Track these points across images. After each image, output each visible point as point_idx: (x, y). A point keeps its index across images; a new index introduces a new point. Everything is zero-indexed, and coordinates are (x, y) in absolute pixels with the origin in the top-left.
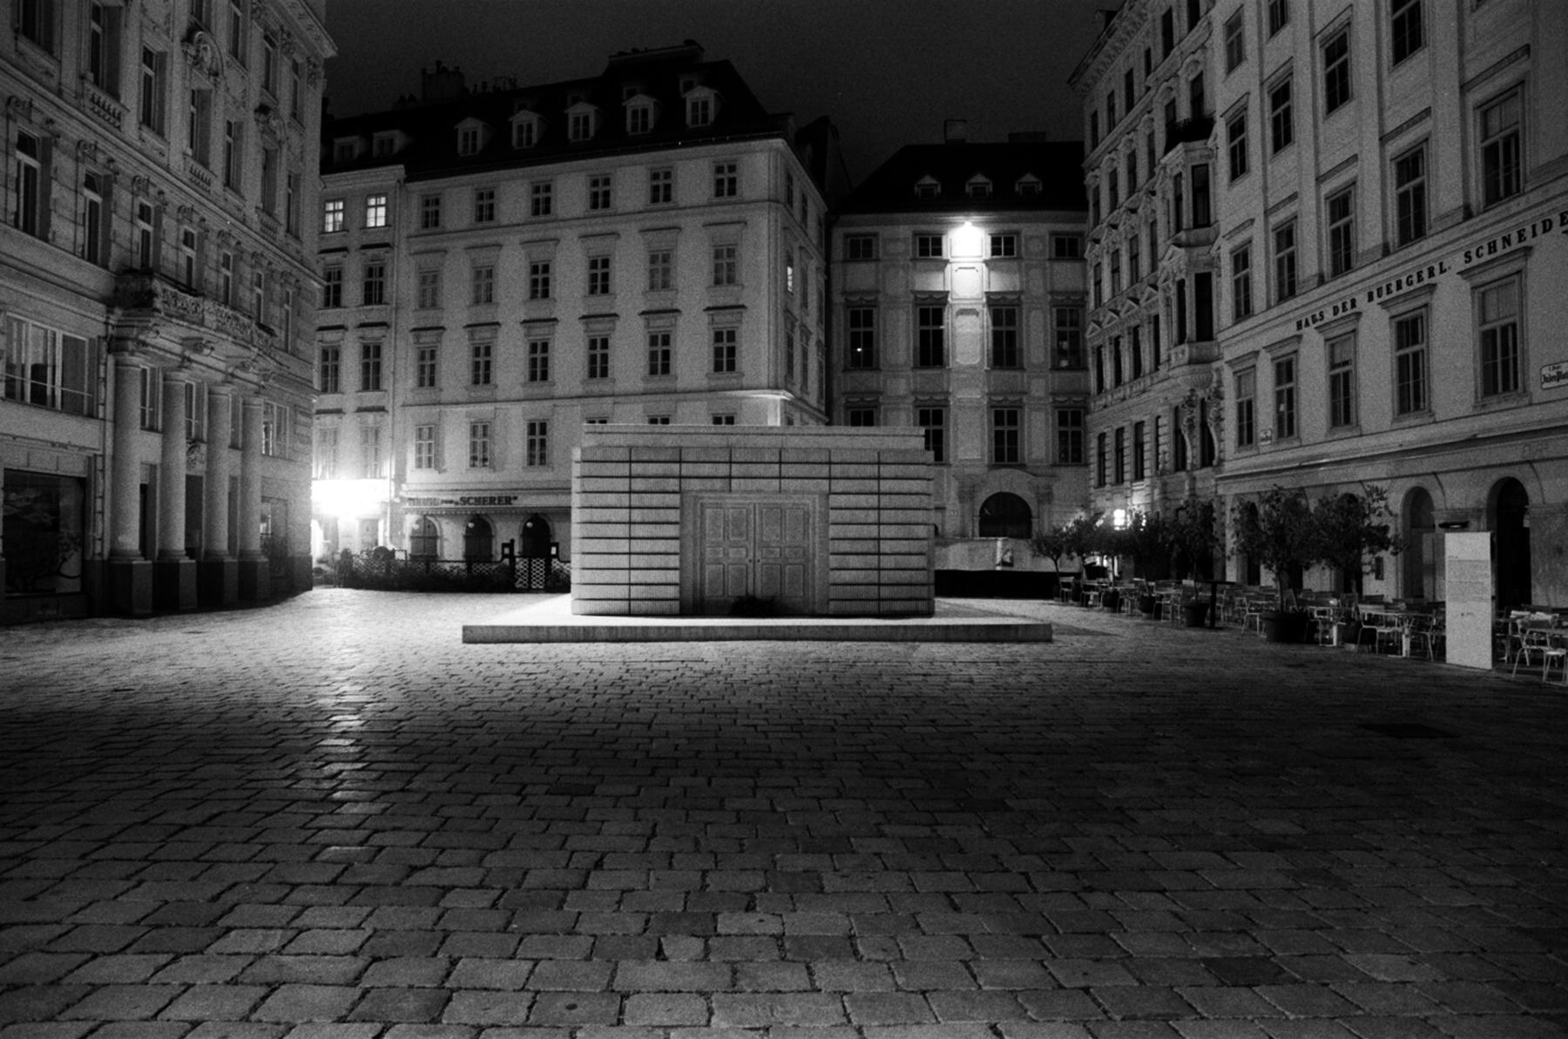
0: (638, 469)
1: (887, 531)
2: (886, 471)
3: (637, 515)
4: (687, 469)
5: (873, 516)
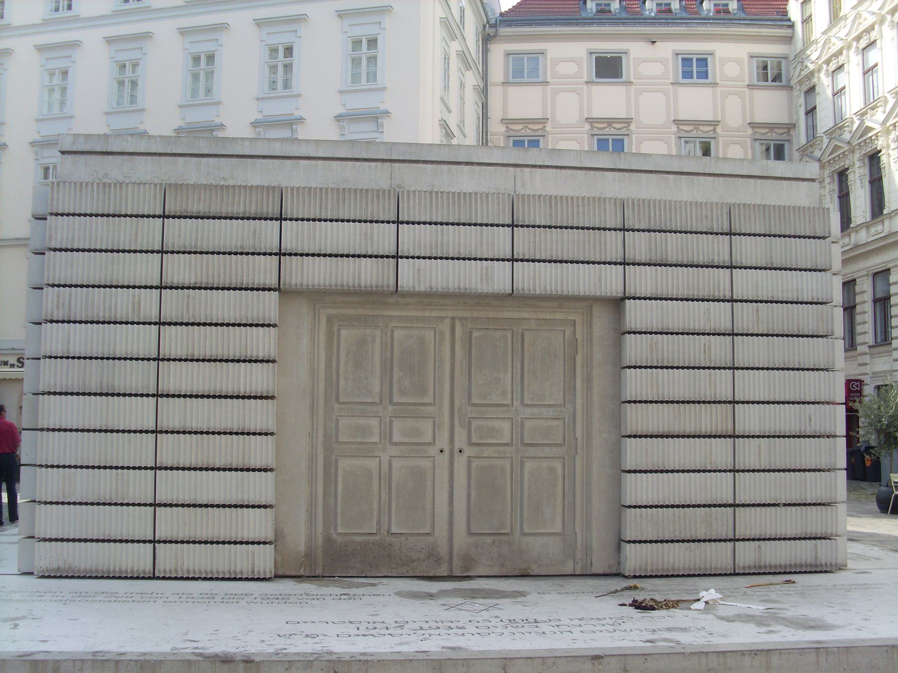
0: (181, 232)
1: (752, 385)
2: (749, 250)
3: (176, 341)
4: (295, 235)
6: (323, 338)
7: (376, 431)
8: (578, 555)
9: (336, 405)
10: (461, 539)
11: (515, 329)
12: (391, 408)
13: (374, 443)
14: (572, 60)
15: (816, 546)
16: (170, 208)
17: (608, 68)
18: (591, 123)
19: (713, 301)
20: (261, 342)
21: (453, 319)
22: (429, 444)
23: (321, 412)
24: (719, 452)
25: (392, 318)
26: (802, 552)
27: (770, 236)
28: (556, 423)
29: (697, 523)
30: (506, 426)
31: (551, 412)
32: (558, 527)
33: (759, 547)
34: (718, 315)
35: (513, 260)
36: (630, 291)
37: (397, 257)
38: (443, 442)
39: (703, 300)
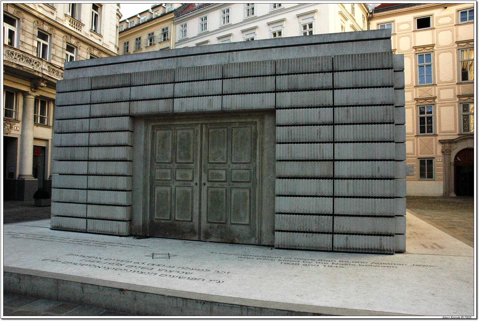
0: (98, 95)
1: (345, 151)
2: (342, 79)
3: (95, 138)
4: (134, 92)
5: (326, 132)
6: (150, 135)
7: (169, 174)
8: (257, 235)
9: (155, 164)
10: (204, 225)
11: (229, 128)
12: (176, 165)
13: (169, 180)
14: (406, 23)
15: (381, 239)
16: (94, 86)
17: (423, 23)
18: (416, 49)
19: (323, 107)
20: (124, 137)
21: (202, 124)
22: (191, 181)
23: (149, 167)
24: (326, 186)
25: (176, 125)
26: (374, 242)
27: (356, 70)
28: (247, 171)
29: (312, 223)
30: (224, 173)
31: (245, 166)
32: (247, 221)
33: (347, 238)
34: (326, 114)
35: (222, 95)
36: (278, 105)
37: (173, 98)
38: (197, 180)
39: (317, 107)
